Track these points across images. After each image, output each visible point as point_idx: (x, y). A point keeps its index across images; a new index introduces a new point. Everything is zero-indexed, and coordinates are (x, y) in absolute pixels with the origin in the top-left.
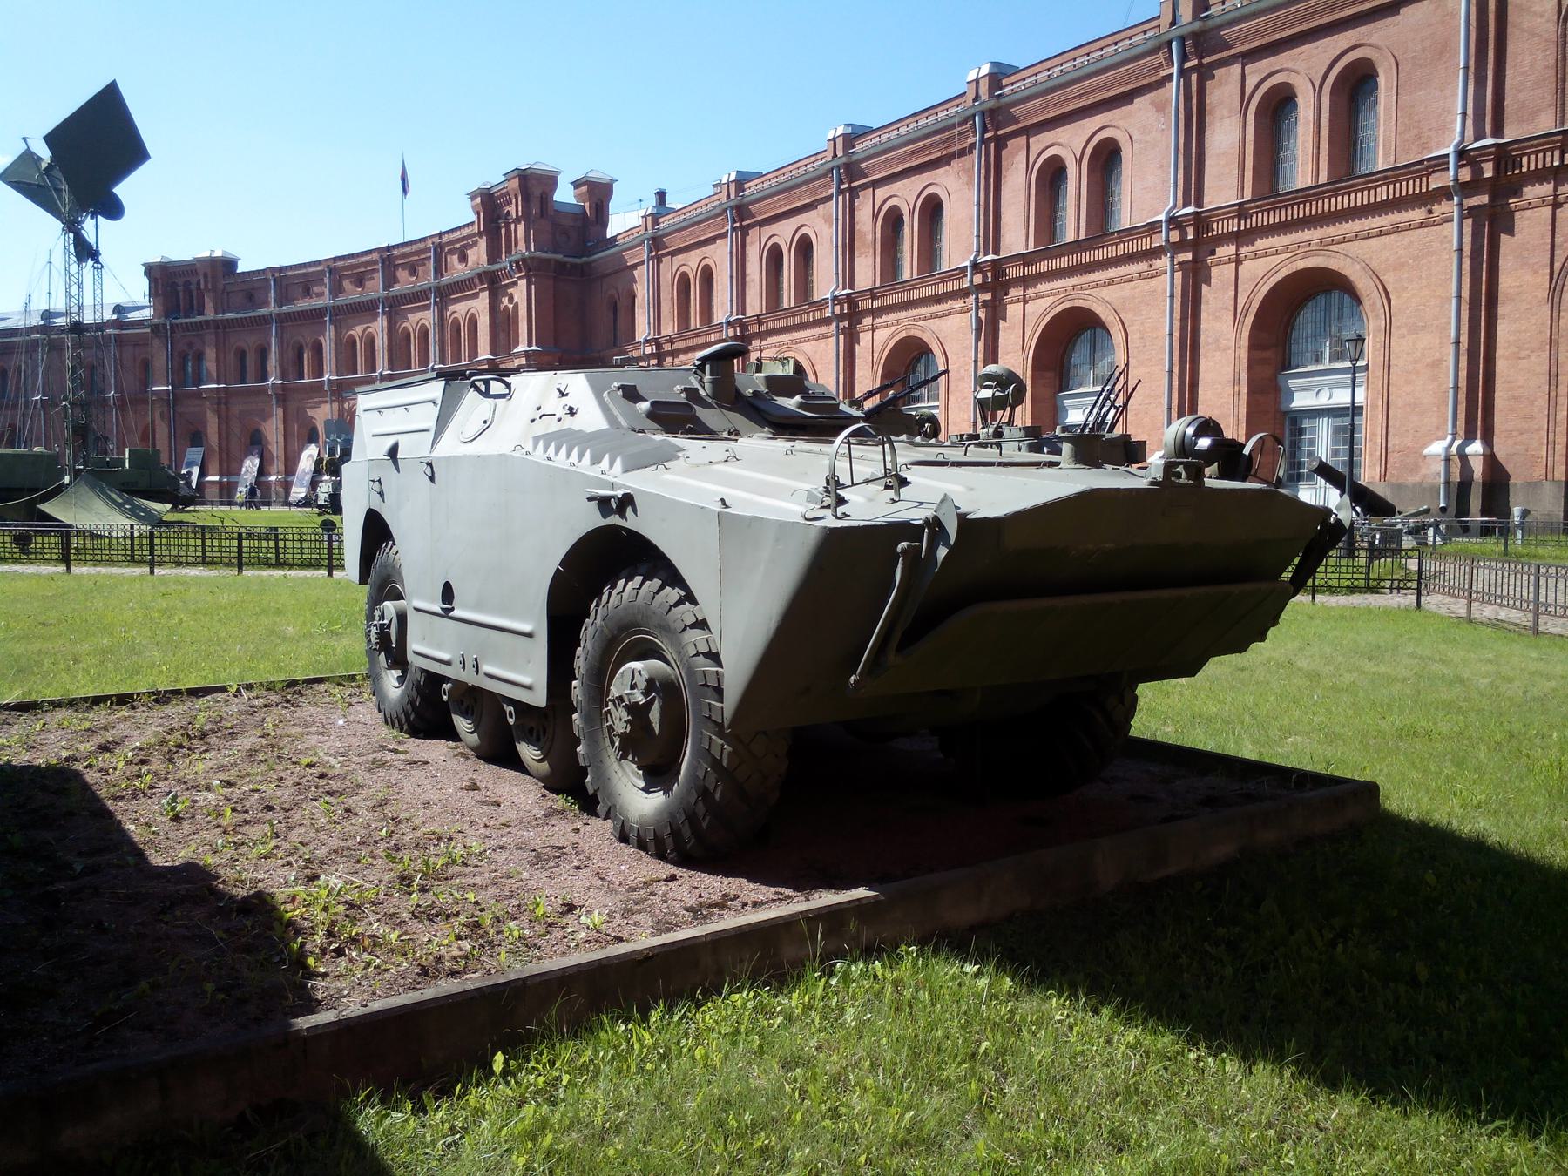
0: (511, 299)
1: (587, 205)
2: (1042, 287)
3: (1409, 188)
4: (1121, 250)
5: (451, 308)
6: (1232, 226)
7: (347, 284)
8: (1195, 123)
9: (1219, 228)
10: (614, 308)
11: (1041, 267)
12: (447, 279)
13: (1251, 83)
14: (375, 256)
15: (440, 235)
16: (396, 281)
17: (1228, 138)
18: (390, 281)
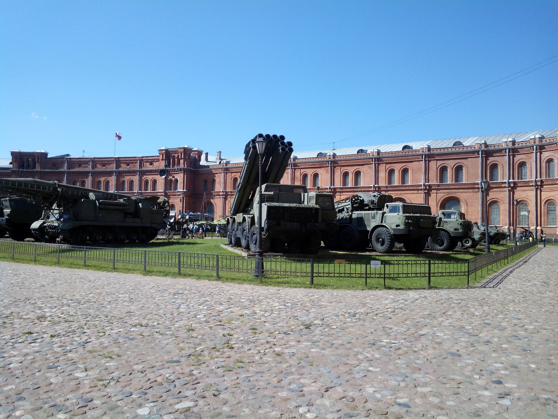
0: (174, 177)
1: (197, 157)
2: (344, 193)
3: (415, 188)
4: (362, 190)
5: (145, 177)
6: (385, 189)
7: (98, 165)
8: (377, 172)
9: (382, 189)
10: (206, 182)
11: (345, 190)
12: (144, 169)
13: (387, 167)
14: (114, 159)
15: (142, 157)
16: (120, 167)
17: (383, 175)
18: (118, 166)
